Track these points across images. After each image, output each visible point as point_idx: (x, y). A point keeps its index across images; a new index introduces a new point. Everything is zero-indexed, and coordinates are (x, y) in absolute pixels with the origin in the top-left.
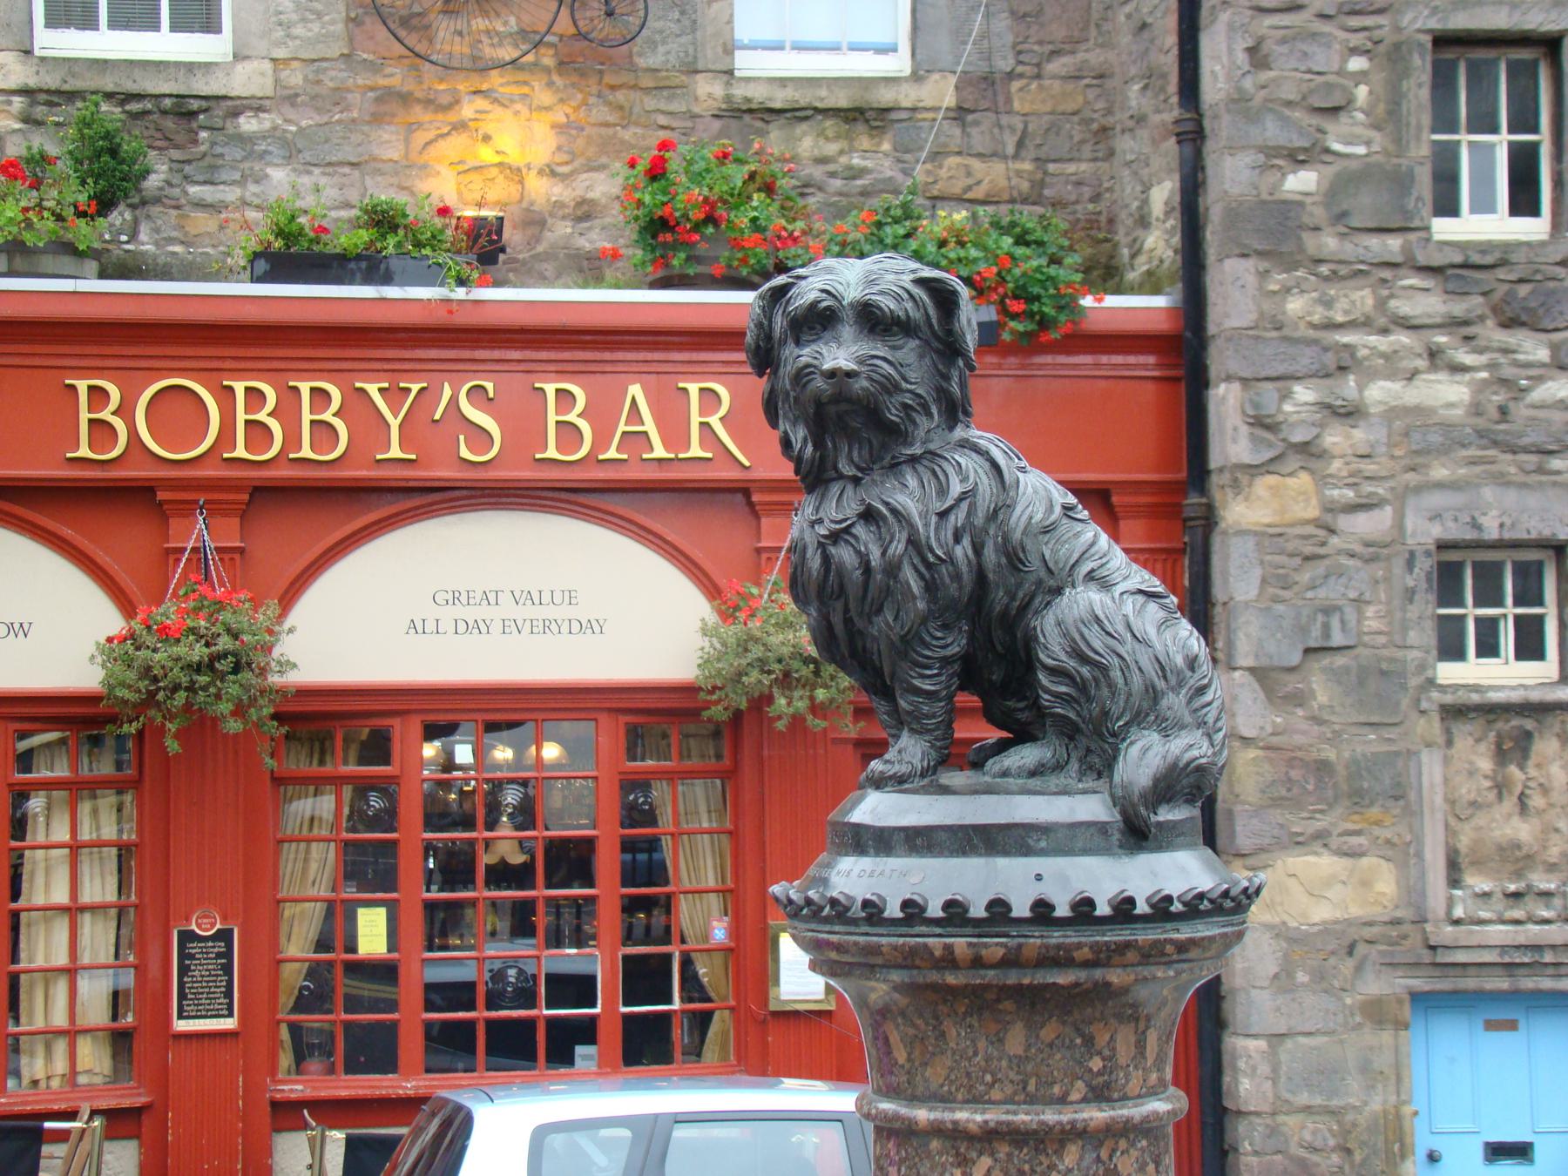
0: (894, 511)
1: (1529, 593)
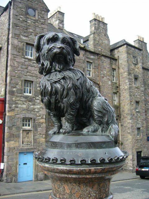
0: (70, 78)
1: (29, 122)
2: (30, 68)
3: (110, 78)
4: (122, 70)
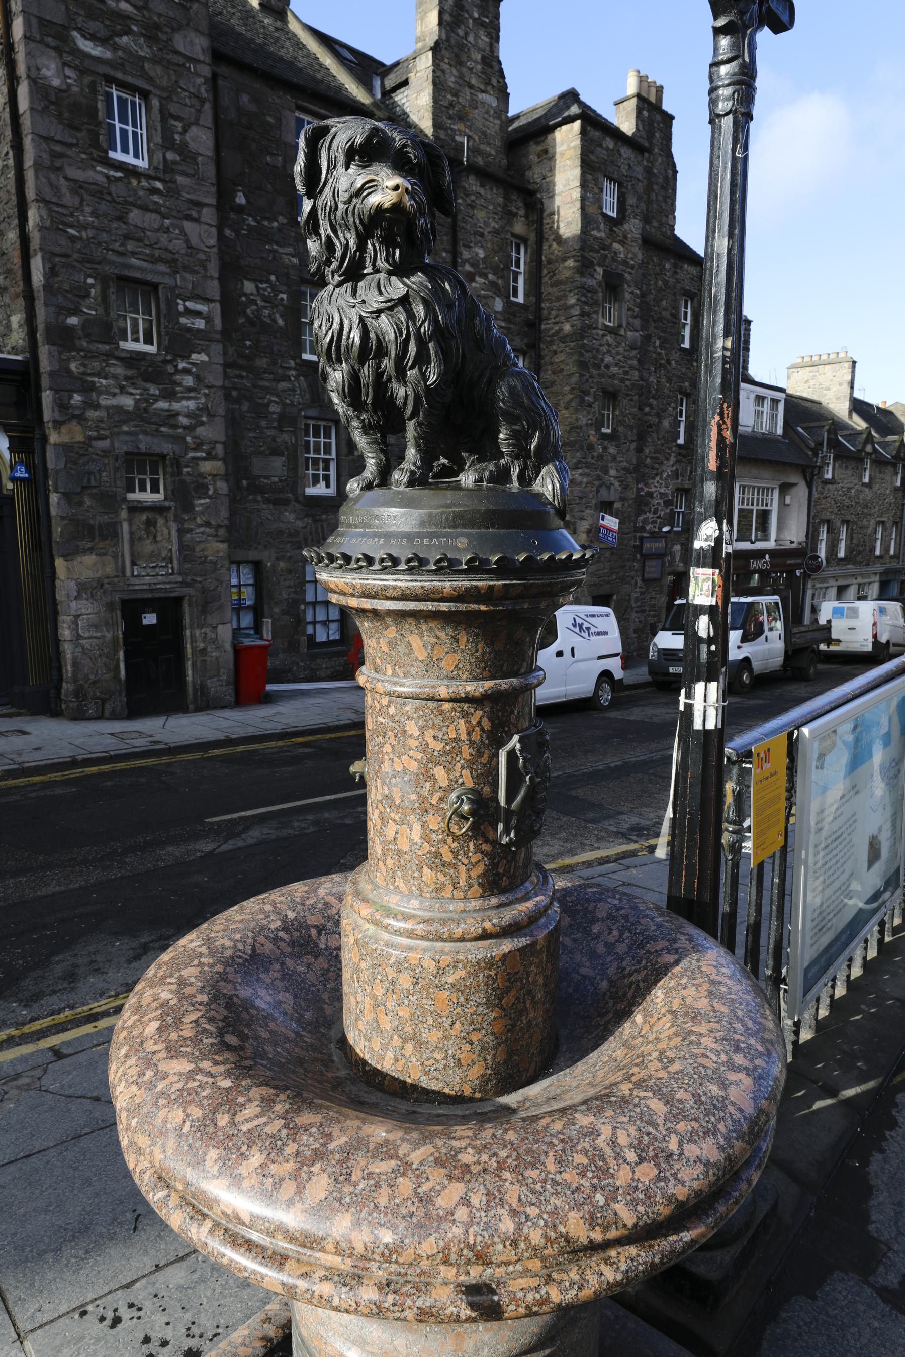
2: (135, 215)
3: (500, 282)
4: (555, 245)
